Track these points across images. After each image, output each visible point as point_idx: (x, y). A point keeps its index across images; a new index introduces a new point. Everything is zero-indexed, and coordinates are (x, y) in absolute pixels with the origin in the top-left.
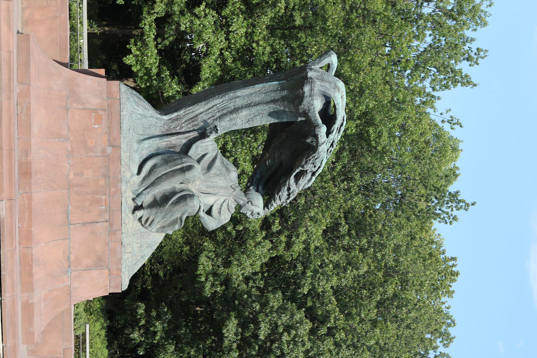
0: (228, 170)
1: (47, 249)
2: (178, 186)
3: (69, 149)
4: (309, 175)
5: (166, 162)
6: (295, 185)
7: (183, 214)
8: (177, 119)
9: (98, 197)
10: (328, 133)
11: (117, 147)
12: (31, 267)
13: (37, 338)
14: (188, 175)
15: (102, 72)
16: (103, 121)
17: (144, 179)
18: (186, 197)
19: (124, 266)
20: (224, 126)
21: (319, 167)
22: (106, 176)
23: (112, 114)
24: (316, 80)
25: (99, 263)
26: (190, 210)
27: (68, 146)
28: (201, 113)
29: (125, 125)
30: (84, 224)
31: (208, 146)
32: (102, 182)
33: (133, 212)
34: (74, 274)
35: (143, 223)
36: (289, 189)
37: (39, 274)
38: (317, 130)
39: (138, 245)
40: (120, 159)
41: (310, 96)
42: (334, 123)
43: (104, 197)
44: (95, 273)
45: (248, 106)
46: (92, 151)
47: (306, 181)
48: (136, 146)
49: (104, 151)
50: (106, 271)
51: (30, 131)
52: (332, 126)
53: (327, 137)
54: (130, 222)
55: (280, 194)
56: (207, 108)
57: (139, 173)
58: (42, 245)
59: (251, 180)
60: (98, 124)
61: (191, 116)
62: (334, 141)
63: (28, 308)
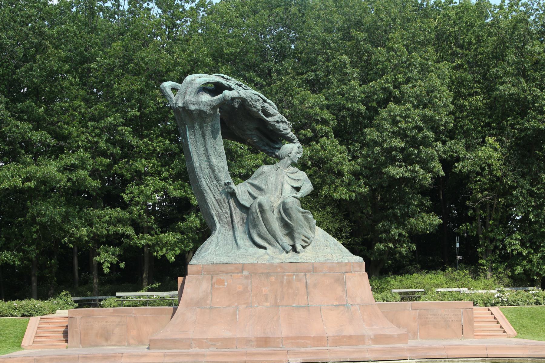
0: (262, 174)
1: (329, 324)
2: (276, 215)
3: (245, 306)
4: (266, 105)
5: (255, 225)
7: (299, 211)
8: (219, 217)
9: (285, 282)
10: (230, 89)
11: (243, 267)
12: (344, 337)
13: (402, 331)
14: (266, 207)
15: (180, 279)
16: (222, 278)
17: (270, 244)
18: (285, 209)
19: (343, 260)
20: (225, 177)
21: (259, 96)
22: (268, 275)
23: (215, 271)
24: (185, 99)
25: (341, 281)
26: (296, 206)
27: (242, 307)
28: (214, 196)
29: (225, 260)
30: (308, 293)
31: (242, 190)
32: (273, 279)
33: (297, 252)
34: (349, 302)
36: (278, 122)
37: (350, 331)
38: (228, 98)
39: (325, 248)
40: (253, 264)
41: (199, 104)
42: (222, 84)
44: (349, 284)
45: (208, 157)
46: (247, 287)
47: (271, 107)
48: (242, 251)
49: (246, 277)
50: (348, 275)
51: (230, 338)
52: (224, 85)
53: (233, 89)
54: (306, 255)
55: (282, 129)
56: (209, 191)
57: (265, 248)
58: (325, 328)
59: (270, 154)
60: (224, 282)
61: (216, 205)
62: (237, 84)
63: (378, 339)
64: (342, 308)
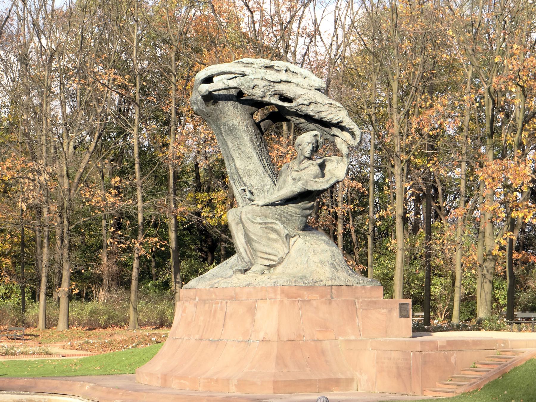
6: (298, 100)
25: (252, 310)
35: (274, 263)
43: (214, 305)
44: (259, 315)
64: (243, 344)
